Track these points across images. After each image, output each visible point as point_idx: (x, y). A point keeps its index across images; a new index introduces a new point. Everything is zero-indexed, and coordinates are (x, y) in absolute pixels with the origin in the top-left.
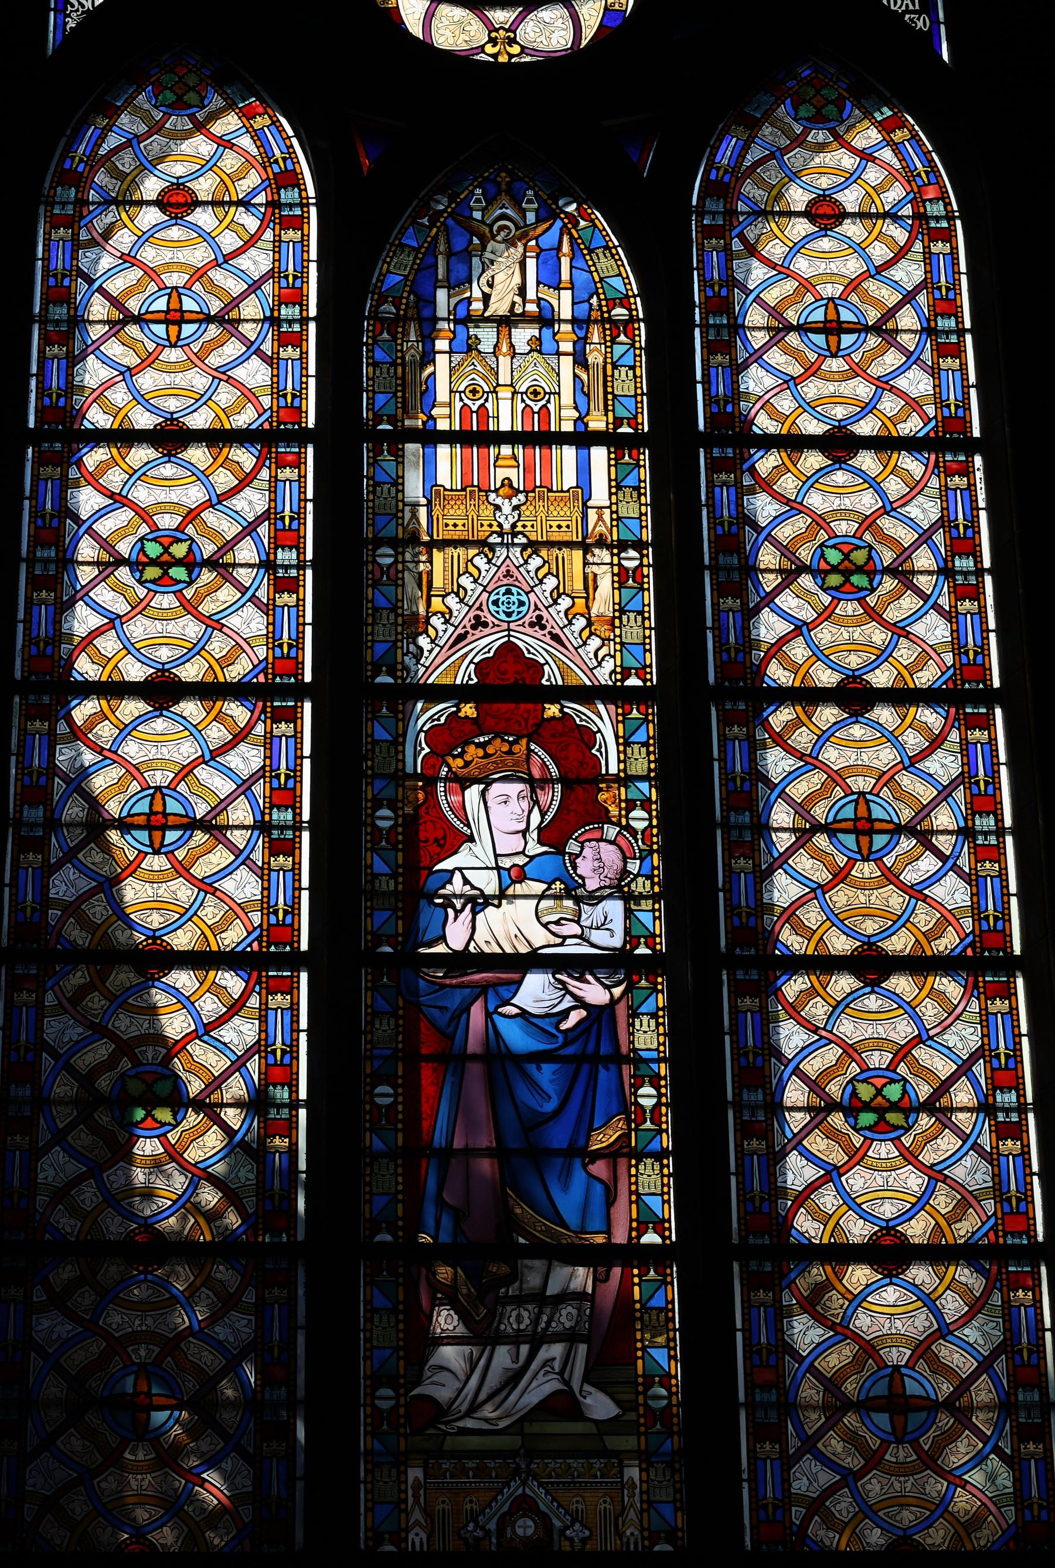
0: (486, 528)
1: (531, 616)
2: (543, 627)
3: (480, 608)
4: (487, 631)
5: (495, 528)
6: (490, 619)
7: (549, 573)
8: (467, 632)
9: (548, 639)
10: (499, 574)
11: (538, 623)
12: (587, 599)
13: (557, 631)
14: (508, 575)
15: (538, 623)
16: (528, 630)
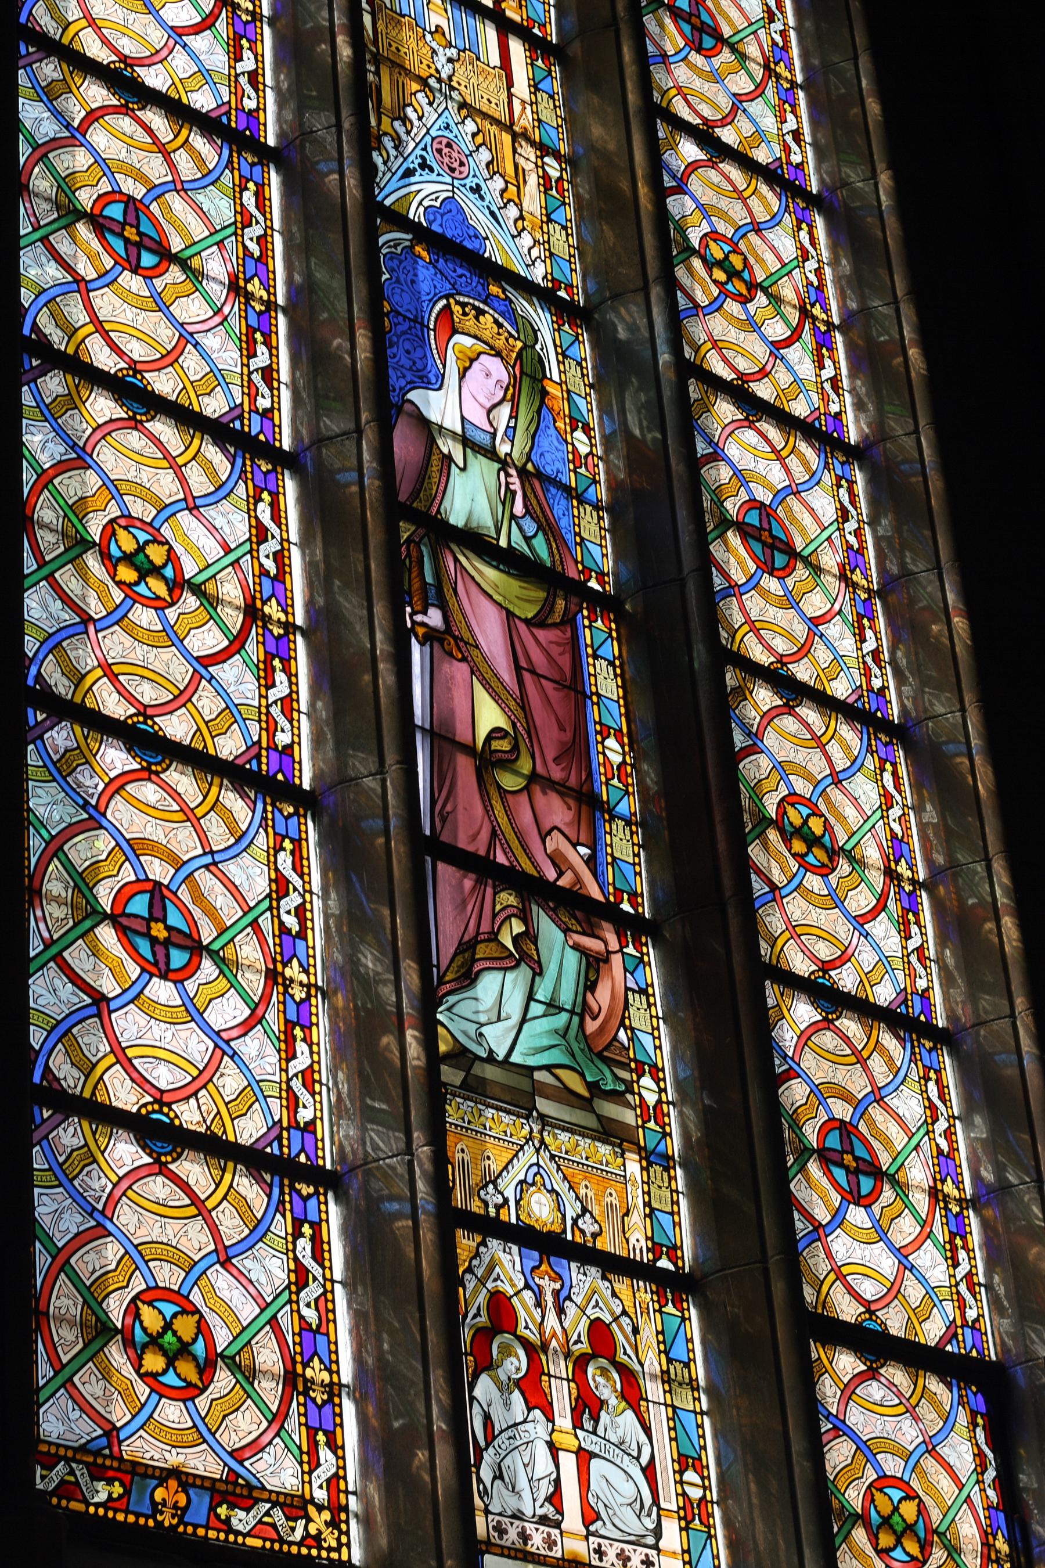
0: (424, 66)
1: (471, 182)
2: (482, 198)
3: (425, 149)
4: (433, 177)
5: (433, 71)
6: (435, 166)
7: (484, 144)
8: (415, 170)
9: (487, 212)
10: (439, 122)
11: (476, 190)
12: (518, 187)
13: (494, 208)
14: (447, 127)
15: (476, 190)
16: (471, 195)
